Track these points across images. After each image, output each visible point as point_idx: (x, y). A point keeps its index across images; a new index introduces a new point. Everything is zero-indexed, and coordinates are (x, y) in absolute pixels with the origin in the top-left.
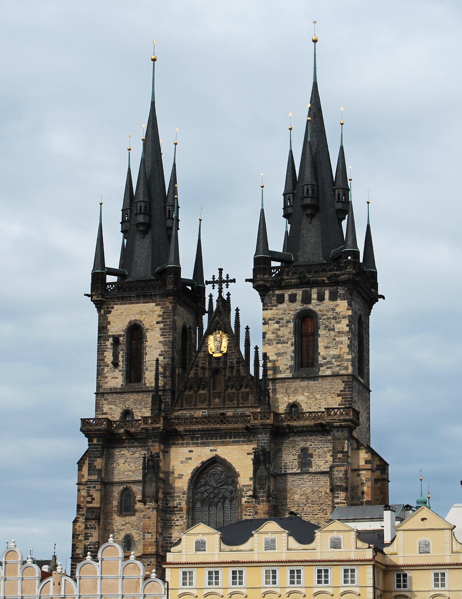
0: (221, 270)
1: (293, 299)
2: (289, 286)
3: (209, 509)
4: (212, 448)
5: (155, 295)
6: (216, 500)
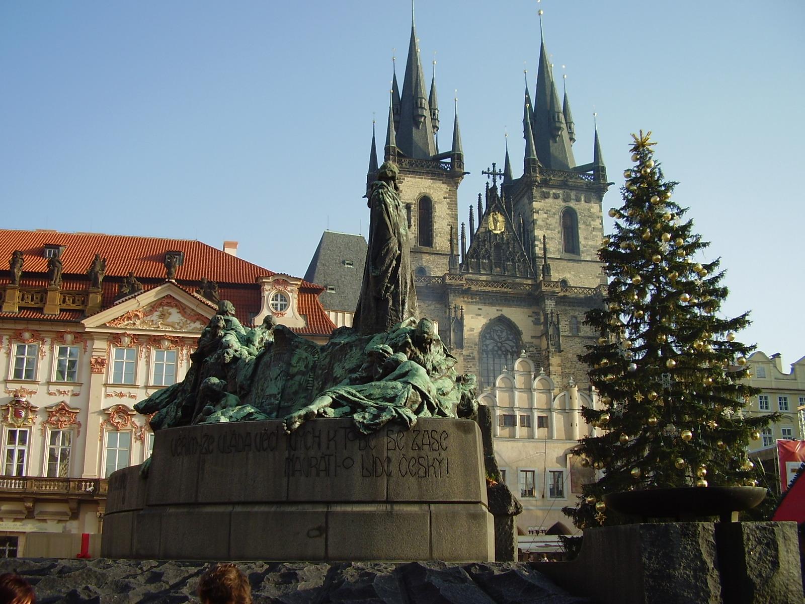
0: (494, 165)
1: (556, 197)
2: (553, 187)
3: (494, 360)
4: (498, 308)
5: (443, 174)
6: (500, 352)
